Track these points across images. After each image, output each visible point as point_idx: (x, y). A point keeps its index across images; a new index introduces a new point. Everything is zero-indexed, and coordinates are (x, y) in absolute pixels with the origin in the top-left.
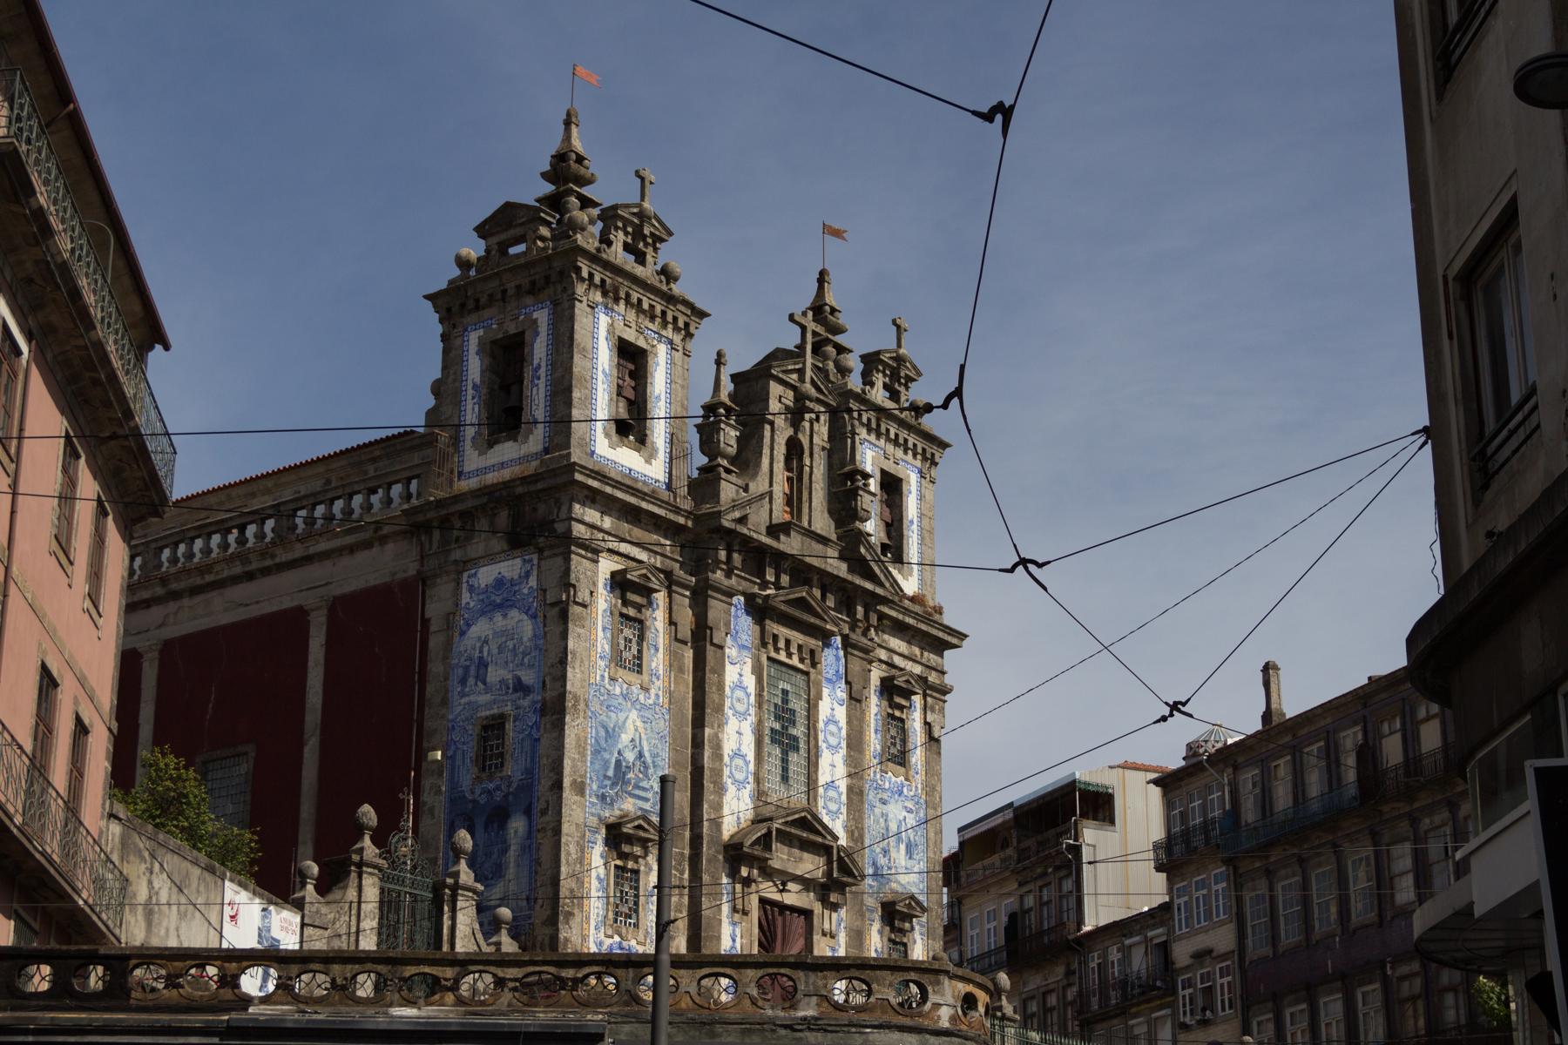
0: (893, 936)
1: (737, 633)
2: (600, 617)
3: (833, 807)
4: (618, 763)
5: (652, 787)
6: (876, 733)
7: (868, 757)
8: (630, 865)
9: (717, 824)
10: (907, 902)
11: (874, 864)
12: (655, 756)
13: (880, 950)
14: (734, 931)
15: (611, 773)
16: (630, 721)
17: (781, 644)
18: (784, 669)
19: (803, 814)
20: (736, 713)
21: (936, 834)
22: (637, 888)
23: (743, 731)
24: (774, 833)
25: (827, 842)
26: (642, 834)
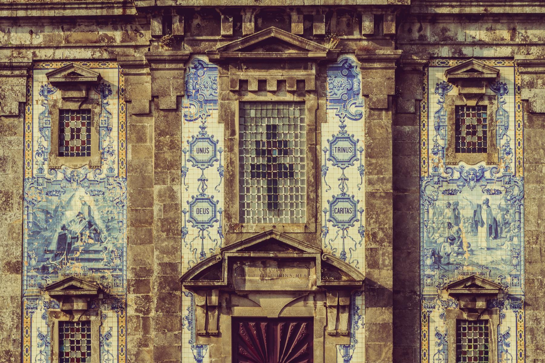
0: (465, 316)
1: (198, 91)
2: (36, 121)
3: (345, 217)
4: (62, 238)
5: (106, 248)
6: (438, 128)
7: (424, 155)
8: (76, 318)
9: (173, 267)
10: (469, 283)
11: (433, 254)
12: (107, 222)
13: (443, 334)
14: (199, 354)
15: (53, 247)
16: (76, 198)
17: (254, 86)
18: (270, 107)
19: (268, 237)
20: (197, 163)
21: (539, 206)
22: (89, 336)
23: (206, 176)
24: (226, 264)
25: (305, 255)
26: (73, 292)
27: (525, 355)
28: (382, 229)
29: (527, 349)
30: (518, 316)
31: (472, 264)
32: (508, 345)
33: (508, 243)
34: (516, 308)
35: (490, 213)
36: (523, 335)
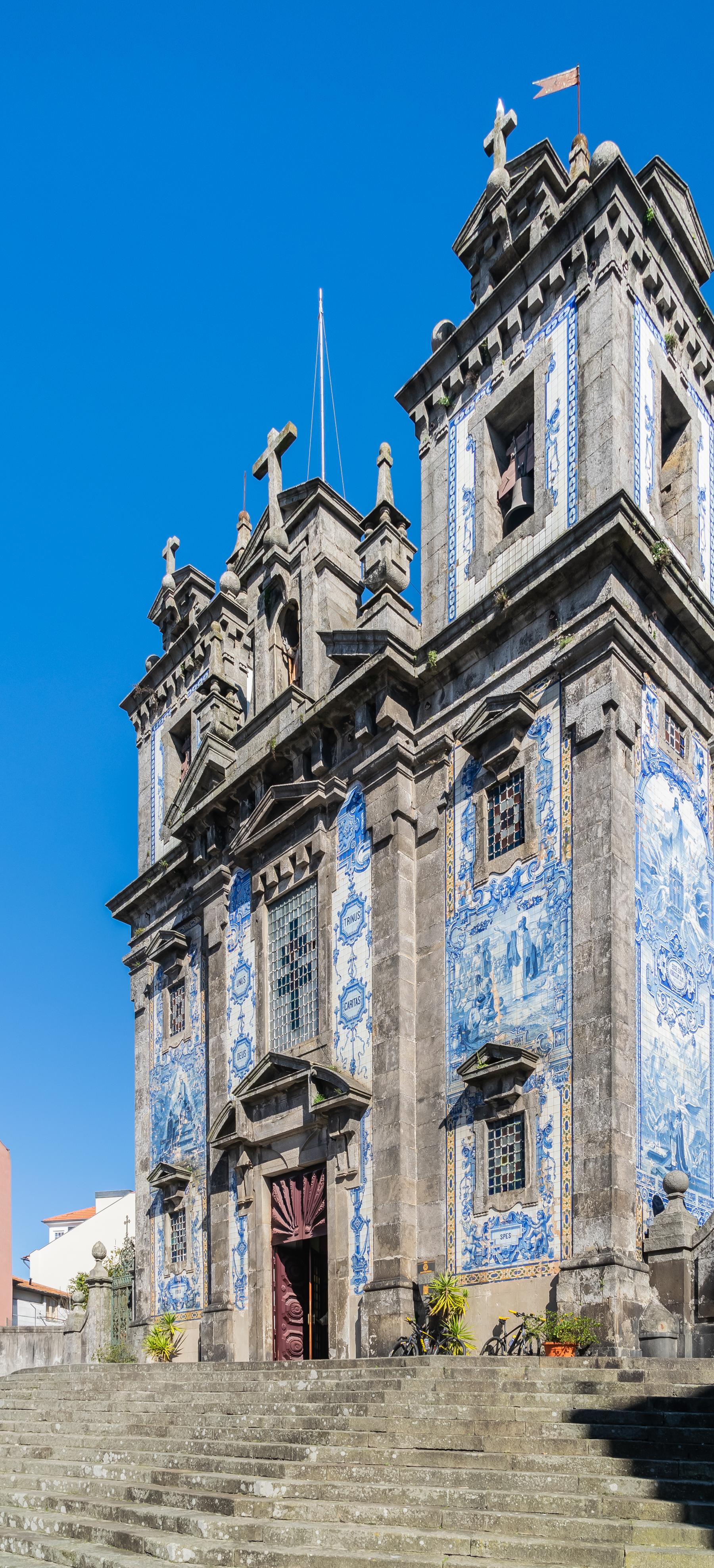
6: (465, 838)
27: (572, 1156)
28: (387, 1013)
29: (575, 1145)
30: (564, 1093)
31: (506, 1029)
32: (549, 1145)
33: (550, 979)
34: (560, 1081)
35: (527, 940)
36: (569, 1123)
